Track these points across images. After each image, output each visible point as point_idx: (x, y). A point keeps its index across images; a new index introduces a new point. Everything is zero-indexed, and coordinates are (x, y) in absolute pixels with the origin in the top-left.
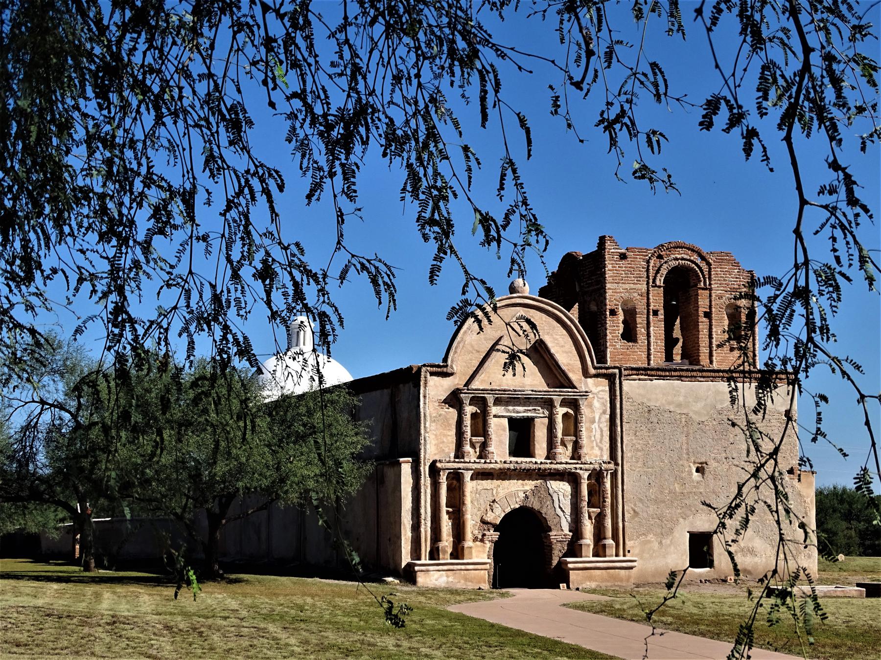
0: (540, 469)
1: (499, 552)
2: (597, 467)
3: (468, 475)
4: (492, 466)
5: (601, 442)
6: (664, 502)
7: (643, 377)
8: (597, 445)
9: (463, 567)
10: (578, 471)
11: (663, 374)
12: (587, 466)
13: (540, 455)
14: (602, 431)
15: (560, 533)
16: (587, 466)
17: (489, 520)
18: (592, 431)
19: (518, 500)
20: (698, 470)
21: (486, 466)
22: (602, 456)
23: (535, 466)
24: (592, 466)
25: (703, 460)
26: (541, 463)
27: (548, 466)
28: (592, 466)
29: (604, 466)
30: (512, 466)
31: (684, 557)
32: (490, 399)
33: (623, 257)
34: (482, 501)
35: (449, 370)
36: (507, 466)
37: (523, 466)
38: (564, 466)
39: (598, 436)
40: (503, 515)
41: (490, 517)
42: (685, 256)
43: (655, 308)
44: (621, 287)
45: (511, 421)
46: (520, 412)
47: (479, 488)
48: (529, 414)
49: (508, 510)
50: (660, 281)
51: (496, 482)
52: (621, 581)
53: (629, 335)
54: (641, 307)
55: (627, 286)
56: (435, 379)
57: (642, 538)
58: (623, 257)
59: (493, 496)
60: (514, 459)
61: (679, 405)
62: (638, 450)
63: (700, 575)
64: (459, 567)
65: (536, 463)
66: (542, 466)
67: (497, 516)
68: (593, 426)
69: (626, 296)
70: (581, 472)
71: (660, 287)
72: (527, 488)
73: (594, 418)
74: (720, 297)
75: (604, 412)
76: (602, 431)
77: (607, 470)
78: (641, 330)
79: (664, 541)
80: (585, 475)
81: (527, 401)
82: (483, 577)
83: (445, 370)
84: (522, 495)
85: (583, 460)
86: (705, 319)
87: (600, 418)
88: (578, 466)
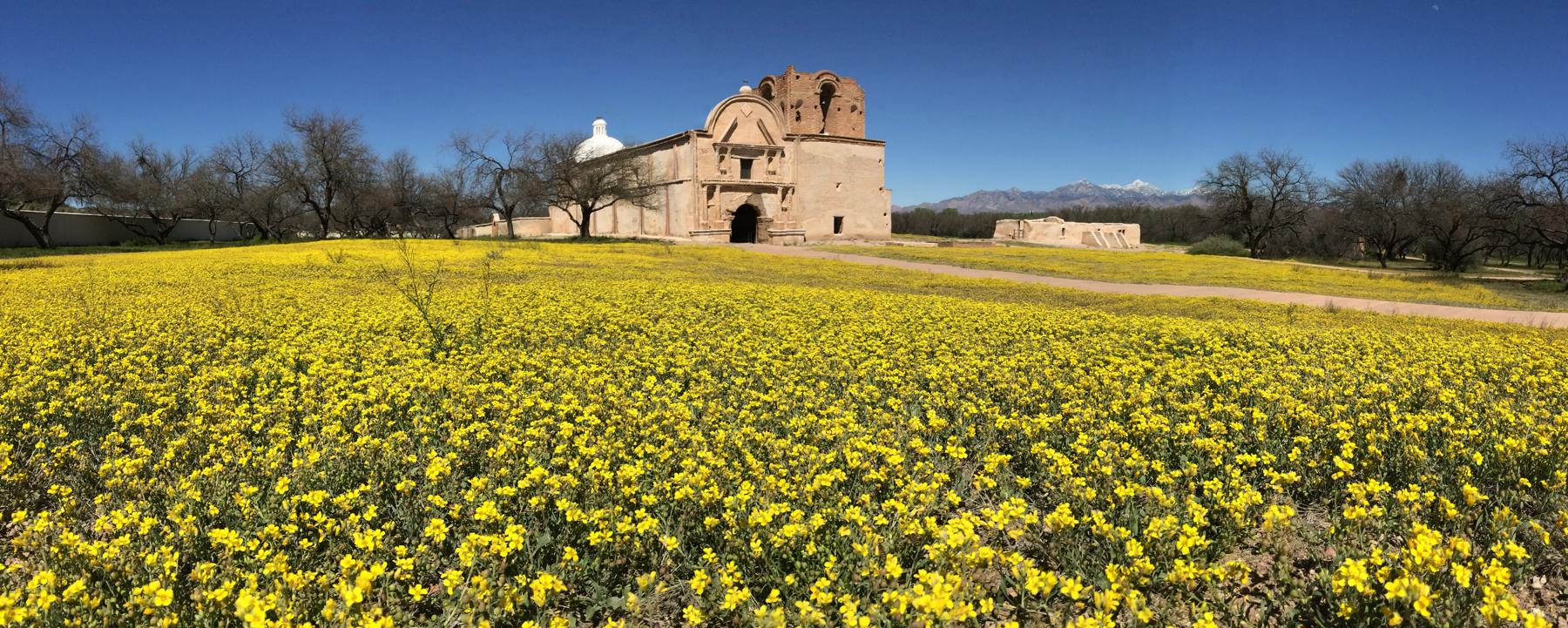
1: (734, 225)
3: (718, 189)
45: (741, 160)
67: (734, 208)
80: (780, 189)
82: (728, 237)
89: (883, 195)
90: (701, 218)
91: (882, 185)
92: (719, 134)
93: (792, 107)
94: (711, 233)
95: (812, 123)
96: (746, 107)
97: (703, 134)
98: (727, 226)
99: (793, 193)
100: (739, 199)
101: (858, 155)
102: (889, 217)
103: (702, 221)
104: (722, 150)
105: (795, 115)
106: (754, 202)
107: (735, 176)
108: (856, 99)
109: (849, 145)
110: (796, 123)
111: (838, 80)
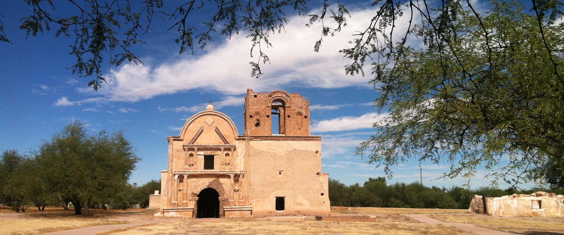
0: (214, 174)
1: (200, 204)
3: (186, 177)
6: (265, 185)
7: (257, 140)
9: (183, 210)
11: (266, 138)
13: (216, 169)
14: (241, 160)
15: (223, 197)
17: (195, 193)
18: (237, 160)
19: (207, 185)
20: (280, 174)
22: (241, 169)
23: (212, 173)
28: (235, 173)
30: (203, 173)
31: (273, 206)
32: (196, 148)
33: (255, 96)
35: (180, 139)
36: (201, 173)
37: (208, 173)
39: (240, 161)
40: (200, 191)
42: (280, 95)
43: (268, 115)
44: (255, 107)
46: (209, 153)
47: (191, 181)
48: (212, 154)
49: (202, 189)
51: (198, 179)
52: (246, 215)
53: (257, 125)
54: (262, 113)
55: (257, 107)
56: (176, 142)
57: (257, 199)
58: (255, 96)
60: (206, 170)
61: (273, 150)
62: (255, 167)
63: (280, 213)
65: (213, 172)
66: (215, 173)
67: (198, 191)
68: (237, 158)
69: (256, 110)
70: (230, 175)
71: (270, 107)
72: (211, 181)
73: (238, 155)
74: (294, 110)
75: (242, 153)
76: (241, 160)
78: (262, 123)
79: (265, 200)
80: (232, 176)
81: (211, 149)
83: (179, 138)
84: (208, 184)
86: (288, 118)
87: (240, 155)
88: (229, 173)
90: (173, 199)
91: (319, 171)
92: (188, 138)
93: (251, 117)
94: (177, 210)
95: (267, 127)
96: (209, 119)
97: (177, 139)
98: (192, 205)
99: (243, 177)
100: (203, 184)
101: (298, 148)
102: (326, 197)
103: (173, 202)
104: (190, 149)
105: (256, 122)
106: (214, 187)
107: (200, 166)
108: (301, 108)
109: (290, 142)
110: (254, 128)
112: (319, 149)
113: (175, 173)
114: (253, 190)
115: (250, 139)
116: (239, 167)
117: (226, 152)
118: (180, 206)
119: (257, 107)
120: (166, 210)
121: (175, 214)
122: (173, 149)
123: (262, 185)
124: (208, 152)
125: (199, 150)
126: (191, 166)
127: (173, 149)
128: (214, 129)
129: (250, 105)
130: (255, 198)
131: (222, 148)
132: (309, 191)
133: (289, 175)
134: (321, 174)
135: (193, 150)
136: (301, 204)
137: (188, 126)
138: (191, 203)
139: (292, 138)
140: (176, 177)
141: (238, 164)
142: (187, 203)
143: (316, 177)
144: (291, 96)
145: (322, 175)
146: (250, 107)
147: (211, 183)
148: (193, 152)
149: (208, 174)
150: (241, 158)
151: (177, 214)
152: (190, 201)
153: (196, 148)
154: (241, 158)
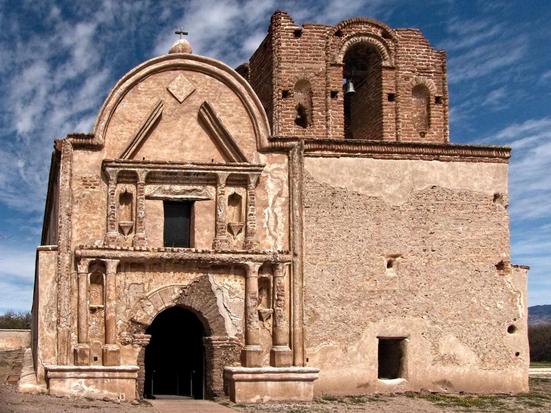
2: (270, 257)
4: (142, 254)
5: (275, 230)
8: (270, 234)
10: (247, 263)
12: (258, 257)
14: (276, 217)
16: (258, 257)
17: (139, 320)
18: (264, 217)
21: (134, 254)
22: (276, 246)
24: (264, 257)
25: (398, 252)
26: (203, 252)
27: (210, 256)
28: (264, 257)
29: (280, 257)
34: (132, 299)
38: (230, 255)
39: (272, 223)
41: (140, 316)
44: (296, 67)
47: (128, 282)
50: (340, 59)
51: (149, 275)
59: (144, 292)
64: (100, 374)
66: (203, 256)
68: (266, 211)
69: (301, 76)
70: (250, 264)
71: (340, 65)
76: (276, 217)
77: (283, 262)
85: (254, 249)
88: (247, 256)
89: (508, 278)
111: (386, 35)
112: (503, 188)
113: (79, 252)
114: (315, 316)
115: (306, 150)
116: (270, 241)
117: (231, 190)
118: (96, 359)
119: (304, 66)
120: (57, 374)
121: (85, 387)
122: (71, 175)
123: (341, 301)
124: (178, 188)
125: (151, 179)
126: (126, 231)
127: (71, 175)
128: (196, 115)
129: (284, 58)
130: (321, 341)
131: (223, 175)
132: (476, 320)
133: (418, 268)
134: (510, 266)
135: (132, 178)
136: (453, 360)
137: (119, 102)
138: (128, 353)
139: (428, 151)
140: (83, 268)
141: (267, 230)
142: (118, 352)
143: (496, 275)
144: (397, 35)
145: (513, 270)
146: (282, 65)
147: (186, 291)
148: (131, 188)
149: (181, 259)
150: (276, 210)
151: (88, 385)
152: (125, 344)
153: (142, 174)
154: (276, 210)
